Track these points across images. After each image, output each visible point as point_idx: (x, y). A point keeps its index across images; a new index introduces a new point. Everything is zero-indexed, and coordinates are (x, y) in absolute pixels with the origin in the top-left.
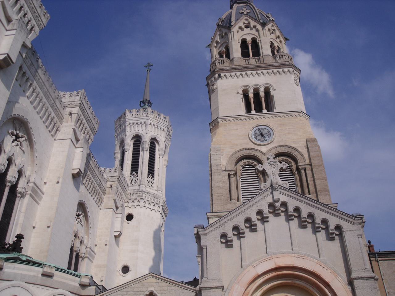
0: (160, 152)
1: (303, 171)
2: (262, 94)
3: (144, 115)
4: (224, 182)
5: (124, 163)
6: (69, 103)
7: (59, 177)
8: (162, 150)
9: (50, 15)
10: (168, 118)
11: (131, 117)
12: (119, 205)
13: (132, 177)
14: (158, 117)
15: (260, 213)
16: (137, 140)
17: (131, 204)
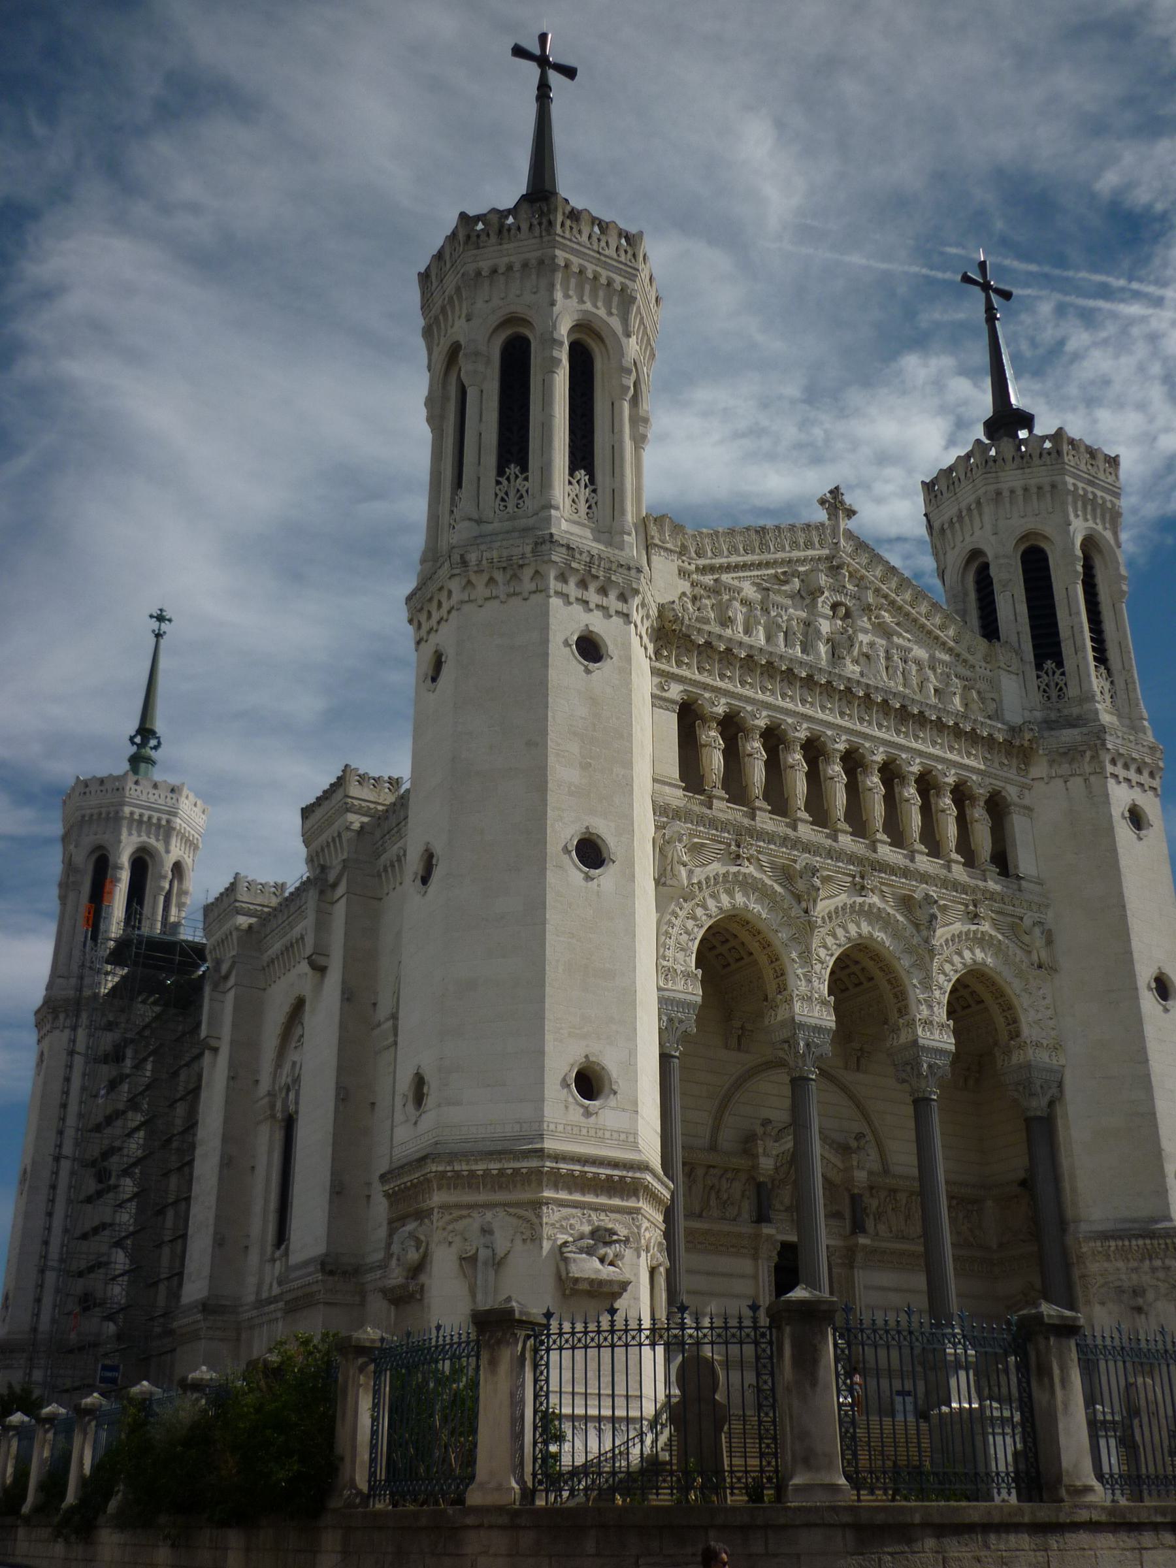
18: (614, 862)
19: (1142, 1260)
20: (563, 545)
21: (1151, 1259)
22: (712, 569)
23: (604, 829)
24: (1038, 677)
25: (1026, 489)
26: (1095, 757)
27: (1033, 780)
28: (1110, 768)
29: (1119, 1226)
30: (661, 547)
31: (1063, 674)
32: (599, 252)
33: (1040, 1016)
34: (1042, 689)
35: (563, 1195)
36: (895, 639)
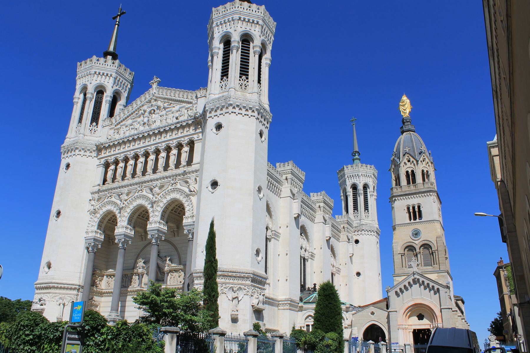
0: (371, 194)
2: (417, 210)
3: (357, 169)
4: (399, 259)
5: (348, 205)
6: (317, 200)
7: (321, 245)
8: (372, 191)
9: (305, 173)
10: (373, 166)
11: (348, 170)
12: (350, 238)
13: (355, 214)
14: (366, 168)
16: (354, 187)
17: (356, 233)
22: (120, 123)
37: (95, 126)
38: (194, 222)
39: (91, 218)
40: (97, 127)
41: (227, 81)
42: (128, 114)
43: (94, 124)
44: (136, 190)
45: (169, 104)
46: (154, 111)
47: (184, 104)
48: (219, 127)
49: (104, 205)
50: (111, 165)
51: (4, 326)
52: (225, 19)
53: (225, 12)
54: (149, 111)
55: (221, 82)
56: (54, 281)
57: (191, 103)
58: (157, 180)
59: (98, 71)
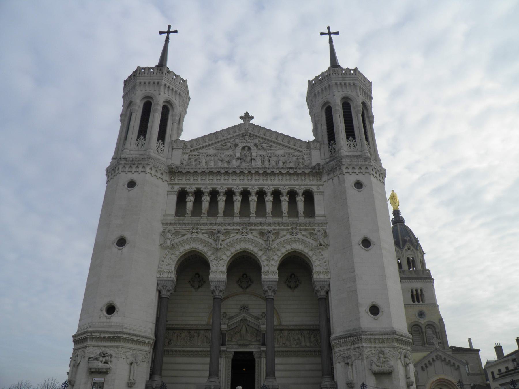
1: (438, 334)
15: (433, 359)
18: (128, 243)
19: (351, 345)
20: (123, 159)
21: (354, 344)
22: (197, 149)
23: (127, 235)
24: (329, 147)
25: (322, 90)
26: (340, 169)
27: (324, 182)
28: (345, 170)
29: (344, 333)
30: (176, 148)
31: (335, 144)
32: (150, 76)
33: (320, 262)
34: (330, 151)
35: (94, 343)
36: (268, 151)
37: (161, 145)
38: (330, 278)
39: (166, 255)
40: (164, 146)
41: (355, 141)
42: (210, 143)
43: (161, 141)
44: (237, 231)
45: (269, 145)
46: (249, 148)
47: (291, 151)
48: (359, 185)
49: (187, 241)
50: (190, 195)
51: (22, 388)
52: (346, 82)
53: (345, 75)
54: (242, 146)
55: (347, 141)
56: (125, 330)
57: (299, 150)
58: (269, 225)
59: (168, 84)
